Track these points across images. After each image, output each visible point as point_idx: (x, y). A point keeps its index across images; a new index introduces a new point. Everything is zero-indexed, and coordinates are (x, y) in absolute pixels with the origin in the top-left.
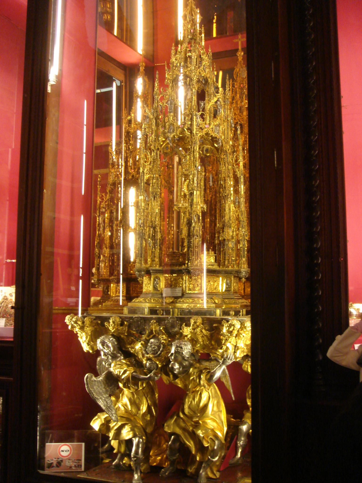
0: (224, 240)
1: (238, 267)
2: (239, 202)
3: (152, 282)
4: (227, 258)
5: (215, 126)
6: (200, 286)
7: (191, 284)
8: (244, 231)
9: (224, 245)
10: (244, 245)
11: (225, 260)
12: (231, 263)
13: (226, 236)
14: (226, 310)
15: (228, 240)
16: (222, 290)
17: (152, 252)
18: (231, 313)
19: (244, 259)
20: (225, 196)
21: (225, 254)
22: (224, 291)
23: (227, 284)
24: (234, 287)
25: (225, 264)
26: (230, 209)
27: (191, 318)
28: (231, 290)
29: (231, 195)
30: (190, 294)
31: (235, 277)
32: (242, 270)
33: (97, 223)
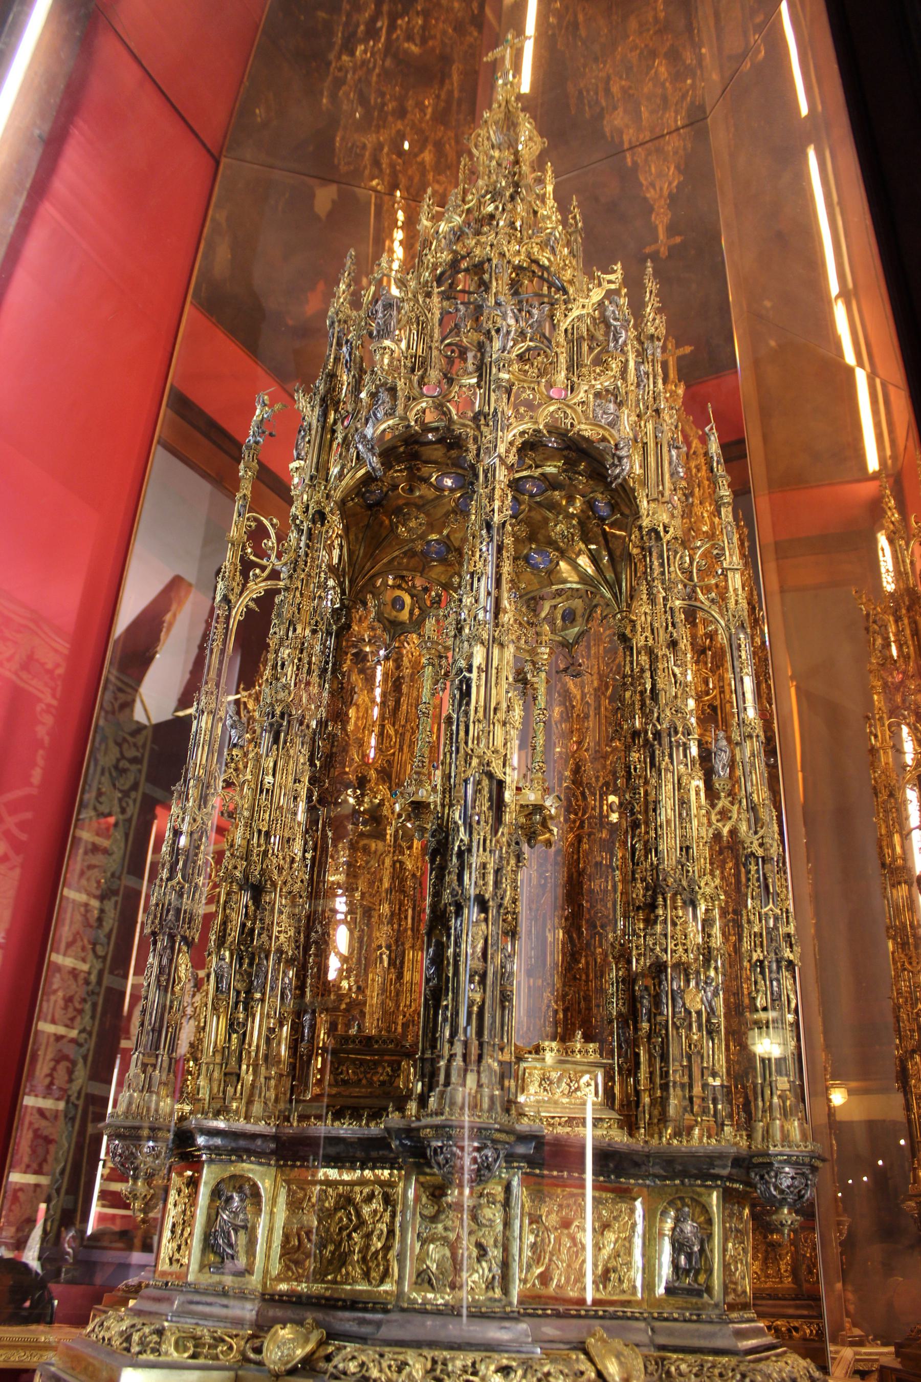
0: (659, 968)
2: (732, 764)
4: (676, 1075)
5: (597, 395)
6: (495, 1253)
7: (432, 1241)
8: (776, 919)
9: (657, 1001)
11: (665, 1087)
12: (705, 1111)
15: (683, 968)
16: (649, 1286)
21: (664, 1057)
23: (678, 1246)
25: (663, 1119)
26: (683, 803)
28: (709, 1290)
30: (423, 1311)
31: (728, 1196)
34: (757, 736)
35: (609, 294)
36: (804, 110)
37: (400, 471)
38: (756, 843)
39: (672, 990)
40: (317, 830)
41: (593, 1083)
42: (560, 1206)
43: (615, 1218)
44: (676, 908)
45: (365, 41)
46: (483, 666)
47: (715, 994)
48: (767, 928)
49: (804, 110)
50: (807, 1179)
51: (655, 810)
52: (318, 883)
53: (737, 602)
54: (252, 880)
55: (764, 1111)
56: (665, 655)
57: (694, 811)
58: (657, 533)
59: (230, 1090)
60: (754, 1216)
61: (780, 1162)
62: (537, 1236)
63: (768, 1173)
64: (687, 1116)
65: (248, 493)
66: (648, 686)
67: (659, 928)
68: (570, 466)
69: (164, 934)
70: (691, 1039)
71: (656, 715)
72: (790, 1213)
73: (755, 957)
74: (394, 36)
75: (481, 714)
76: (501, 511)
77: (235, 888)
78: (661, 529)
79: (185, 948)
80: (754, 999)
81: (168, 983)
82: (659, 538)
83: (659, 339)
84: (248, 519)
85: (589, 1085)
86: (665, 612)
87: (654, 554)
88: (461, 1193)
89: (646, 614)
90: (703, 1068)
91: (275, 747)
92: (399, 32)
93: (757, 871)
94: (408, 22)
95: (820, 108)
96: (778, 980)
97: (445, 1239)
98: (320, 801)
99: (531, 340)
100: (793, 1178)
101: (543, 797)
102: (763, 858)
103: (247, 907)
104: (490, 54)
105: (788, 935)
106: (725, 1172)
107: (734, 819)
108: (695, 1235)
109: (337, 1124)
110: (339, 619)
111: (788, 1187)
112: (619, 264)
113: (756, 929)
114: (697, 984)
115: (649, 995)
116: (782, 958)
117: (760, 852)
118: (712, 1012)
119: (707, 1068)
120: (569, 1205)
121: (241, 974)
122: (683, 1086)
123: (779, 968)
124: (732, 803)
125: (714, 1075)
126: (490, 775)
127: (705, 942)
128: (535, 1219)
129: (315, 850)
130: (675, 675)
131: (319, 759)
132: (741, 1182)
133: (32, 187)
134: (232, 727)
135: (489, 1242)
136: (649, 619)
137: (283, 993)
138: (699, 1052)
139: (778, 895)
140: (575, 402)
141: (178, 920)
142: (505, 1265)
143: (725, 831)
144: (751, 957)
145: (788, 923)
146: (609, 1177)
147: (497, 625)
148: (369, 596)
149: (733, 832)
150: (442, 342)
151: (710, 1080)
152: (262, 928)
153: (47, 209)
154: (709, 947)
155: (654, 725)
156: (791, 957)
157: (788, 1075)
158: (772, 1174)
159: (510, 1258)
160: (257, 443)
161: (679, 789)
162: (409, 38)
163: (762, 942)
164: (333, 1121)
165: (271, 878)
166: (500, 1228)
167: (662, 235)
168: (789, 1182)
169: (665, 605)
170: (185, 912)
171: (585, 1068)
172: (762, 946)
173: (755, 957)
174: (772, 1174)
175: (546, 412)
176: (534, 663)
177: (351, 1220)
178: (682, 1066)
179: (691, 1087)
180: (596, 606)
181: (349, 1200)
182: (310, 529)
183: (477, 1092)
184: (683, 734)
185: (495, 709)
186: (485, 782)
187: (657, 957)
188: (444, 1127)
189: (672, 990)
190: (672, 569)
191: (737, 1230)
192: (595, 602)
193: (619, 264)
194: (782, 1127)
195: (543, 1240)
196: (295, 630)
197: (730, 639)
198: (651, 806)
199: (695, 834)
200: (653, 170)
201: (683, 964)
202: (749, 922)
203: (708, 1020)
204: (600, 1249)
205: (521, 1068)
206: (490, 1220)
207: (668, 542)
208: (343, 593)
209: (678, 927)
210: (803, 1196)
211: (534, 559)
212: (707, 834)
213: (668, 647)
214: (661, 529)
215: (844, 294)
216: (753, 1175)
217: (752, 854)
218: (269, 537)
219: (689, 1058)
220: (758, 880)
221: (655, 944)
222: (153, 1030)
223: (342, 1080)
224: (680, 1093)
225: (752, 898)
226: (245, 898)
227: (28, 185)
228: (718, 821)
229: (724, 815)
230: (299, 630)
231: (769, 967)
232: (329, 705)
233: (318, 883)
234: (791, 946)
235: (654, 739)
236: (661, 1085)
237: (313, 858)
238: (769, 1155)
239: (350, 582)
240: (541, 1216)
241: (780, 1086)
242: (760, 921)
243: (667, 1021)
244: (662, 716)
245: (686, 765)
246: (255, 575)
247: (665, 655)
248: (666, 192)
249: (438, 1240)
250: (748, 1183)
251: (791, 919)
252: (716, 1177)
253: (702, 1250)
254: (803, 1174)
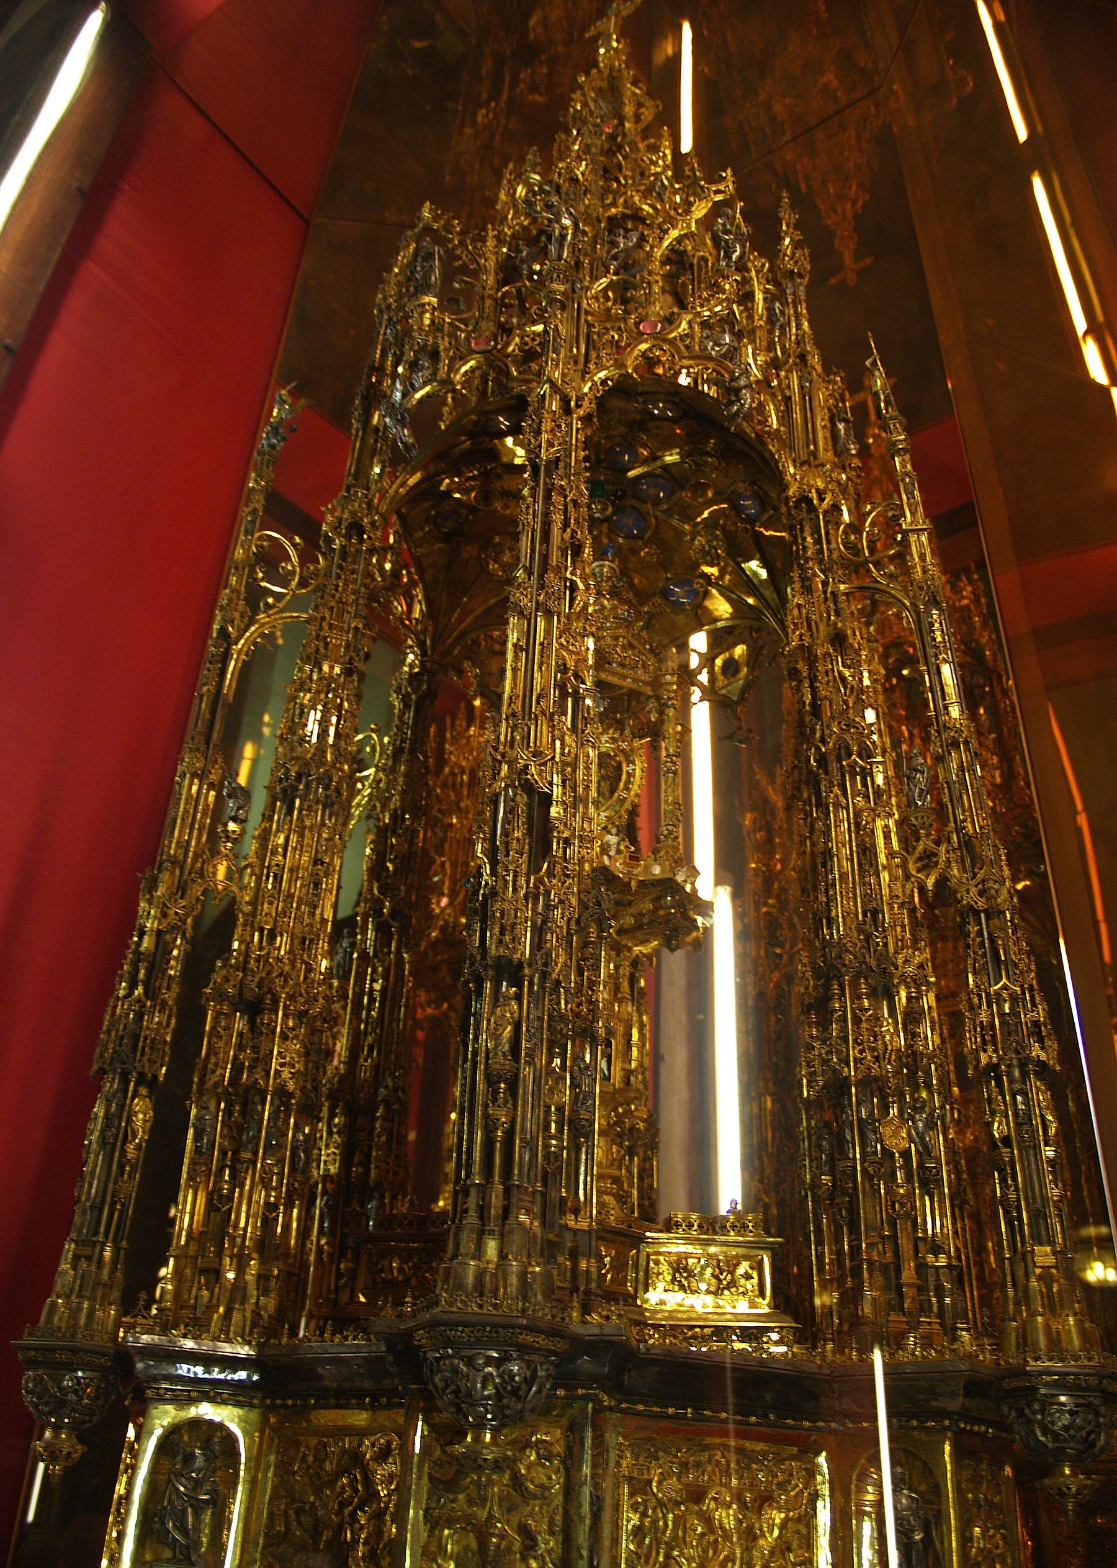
1: (998, 1347)
8: (1014, 999)
10: (1024, 1121)
11: (856, 1271)
12: (924, 1308)
26: (867, 851)
29: (867, 753)
34: (966, 743)
35: (717, 210)
36: (1022, 134)
37: (473, 478)
38: (974, 890)
39: (860, 1119)
40: (390, 952)
41: (755, 1275)
42: (684, 1465)
43: (780, 1486)
44: (859, 998)
45: (486, 105)
46: (523, 643)
47: (930, 1125)
48: (1001, 1015)
49: (1022, 134)
50: (1097, 1414)
51: (824, 865)
52: (390, 1024)
53: (925, 571)
54: (248, 995)
55: (1017, 1303)
56: (827, 654)
57: (882, 859)
60: (1021, 1480)
61: (1047, 1385)
62: (644, 1515)
63: (1029, 1406)
64: (893, 1317)
65: (260, 508)
66: (808, 699)
68: (693, 447)
69: (114, 1071)
70: (895, 1194)
71: (818, 735)
72: (1074, 1474)
73: (984, 1059)
74: (518, 91)
75: (518, 707)
76: (550, 444)
77: (226, 1009)
78: (814, 495)
79: (143, 1091)
80: (989, 1125)
81: (116, 1140)
82: (812, 509)
83: (801, 276)
84: (259, 538)
85: (748, 1277)
86: (826, 599)
87: (806, 534)
88: (478, 1439)
89: (799, 606)
90: (917, 1239)
91: (288, 818)
92: (522, 86)
93: (980, 933)
94: (533, 73)
95: (1040, 128)
96: (1025, 1094)
97: (468, 1519)
98: (393, 913)
99: (614, 274)
100: (1072, 1413)
101: (672, 870)
102: (986, 911)
104: (592, 28)
105: (1036, 1024)
106: (954, 1405)
107: (941, 865)
108: (916, 1516)
109: (338, 1338)
110: (420, 686)
111: (1066, 1428)
112: (729, 171)
113: (983, 1017)
114: (901, 1112)
115: (830, 1134)
116: (1028, 1058)
117: (981, 903)
118: (926, 1151)
119: (925, 1239)
120: (698, 1464)
121: (230, 1128)
122: (884, 1268)
123: (1025, 1075)
124: (938, 843)
125: (936, 1249)
126: (529, 788)
127: (908, 1046)
128: (640, 1487)
129: (386, 978)
130: (843, 679)
131: (391, 861)
132: (989, 1424)
133: (68, 243)
134: (230, 796)
135: (539, 1525)
136: (804, 611)
137: (294, 1154)
138: (907, 1215)
139: (1016, 965)
140: (678, 345)
141: (134, 1049)
143: (930, 883)
144: (978, 1060)
145: (1034, 1005)
146: (766, 1416)
147: (542, 587)
148: (466, 665)
150: (498, 290)
151: (930, 1258)
152: (256, 1060)
153: (92, 271)
154: (914, 1053)
155: (818, 749)
156: (1043, 1056)
157: (1051, 1243)
158: (1036, 1407)
159: (575, 1554)
160: (272, 447)
161: (857, 833)
162: (534, 88)
163: (994, 1036)
164: (333, 1334)
165: (270, 990)
166: (560, 1499)
167: (848, 260)
168: (1066, 1419)
169: (825, 592)
170: (146, 1038)
171: (741, 1251)
172: (994, 1043)
173: (984, 1059)
174: (1036, 1407)
175: (636, 353)
176: (658, 698)
177: (356, 1490)
178: (883, 1237)
179: (898, 1271)
180: (762, 648)
181: (355, 1458)
182: (343, 547)
183: (498, 1266)
184: (860, 756)
185: (539, 697)
186: (522, 799)
187: (834, 1070)
188: (441, 1323)
189: (860, 1119)
190: (834, 546)
191: (992, 1506)
192: (760, 643)
193: (729, 171)
194: (1047, 1326)
195: (655, 1522)
196: (320, 670)
197: (918, 623)
198: (819, 860)
199: (885, 891)
200: (832, 190)
201: (876, 1079)
202: (972, 1008)
203: (920, 1165)
204: (755, 1538)
205: (643, 1255)
206: (542, 1486)
207: (825, 512)
208: (424, 653)
209: (864, 1025)
210: (1093, 1444)
211: (674, 593)
213: (832, 642)
214: (814, 495)
215: (1093, 330)
216: (1005, 1409)
217: (971, 908)
218: (288, 559)
219: (893, 1225)
220: (982, 945)
221: (829, 1052)
222: (92, 1207)
223: (384, 1280)
224: (879, 1279)
225: (975, 973)
226: (240, 1023)
227: (63, 241)
228: (918, 871)
230: (326, 668)
231: (1009, 1074)
232: (404, 792)
233: (390, 1024)
234: (1041, 1040)
235: (818, 768)
236: (851, 1269)
237: (384, 989)
238: (1028, 1373)
239: (432, 641)
240: (650, 1482)
241: (1040, 1261)
242: (989, 1006)
243: (855, 1168)
244: (827, 732)
245: (866, 796)
246: (267, 604)
247: (827, 654)
248: (850, 215)
249: (457, 1520)
250: (1002, 1426)
251: (1038, 999)
252: (942, 1414)
253: (927, 1540)
254: (1089, 1406)
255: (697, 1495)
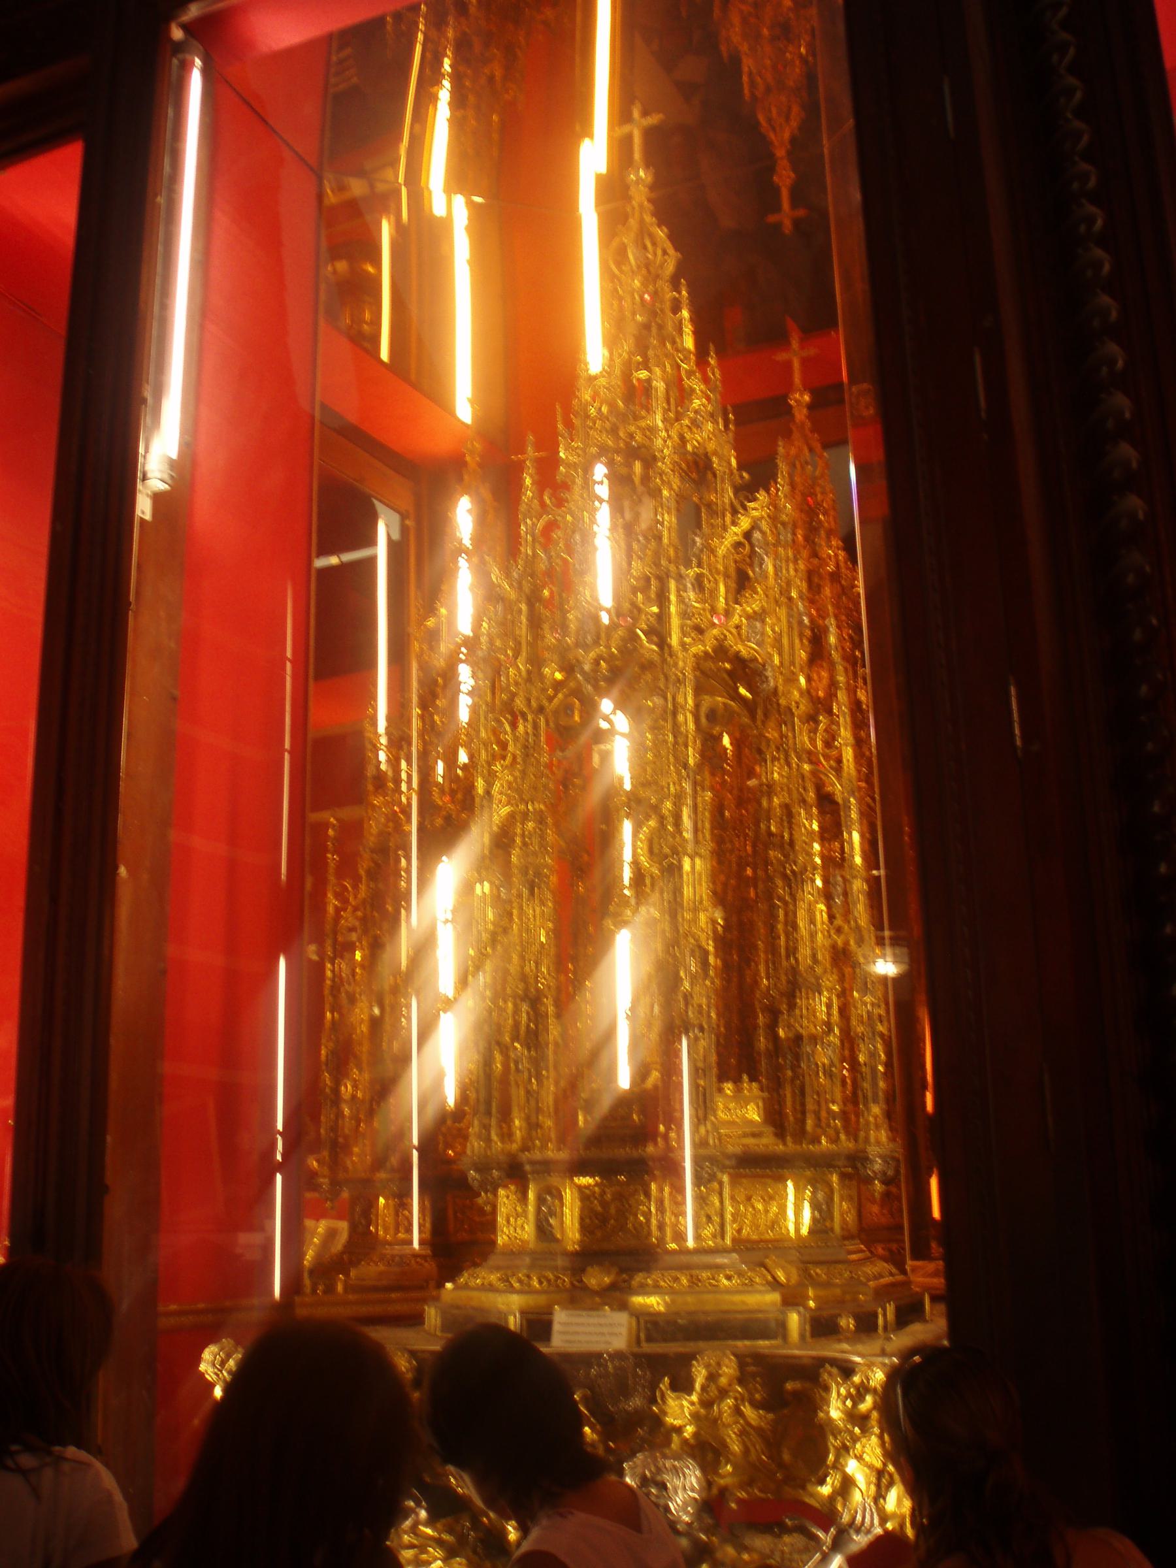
0: (798, 1038)
1: (856, 1141)
2: (846, 894)
3: (531, 1208)
4: (810, 1106)
5: (748, 617)
6: (716, 1219)
8: (873, 1004)
9: (797, 1057)
11: (804, 1113)
12: (829, 1125)
13: (805, 1022)
14: (825, 1313)
15: (814, 1039)
16: (797, 1230)
17: (528, 1092)
18: (843, 1322)
19: (876, 1110)
20: (793, 871)
22: (805, 1231)
23: (815, 1206)
24: (842, 1215)
26: (812, 921)
27: (693, 1356)
31: (843, 1176)
32: (873, 1151)
33: (328, 982)
57: (819, 926)
58: (790, 710)
59: (534, 1133)
67: (797, 1012)
103: (528, 1013)
135: (712, 1212)
142: (722, 1226)
149: (847, 943)
186: (697, 950)
212: (827, 943)
229: (839, 930)
230: (537, 806)
234: (881, 1022)
255: (749, 1199)
